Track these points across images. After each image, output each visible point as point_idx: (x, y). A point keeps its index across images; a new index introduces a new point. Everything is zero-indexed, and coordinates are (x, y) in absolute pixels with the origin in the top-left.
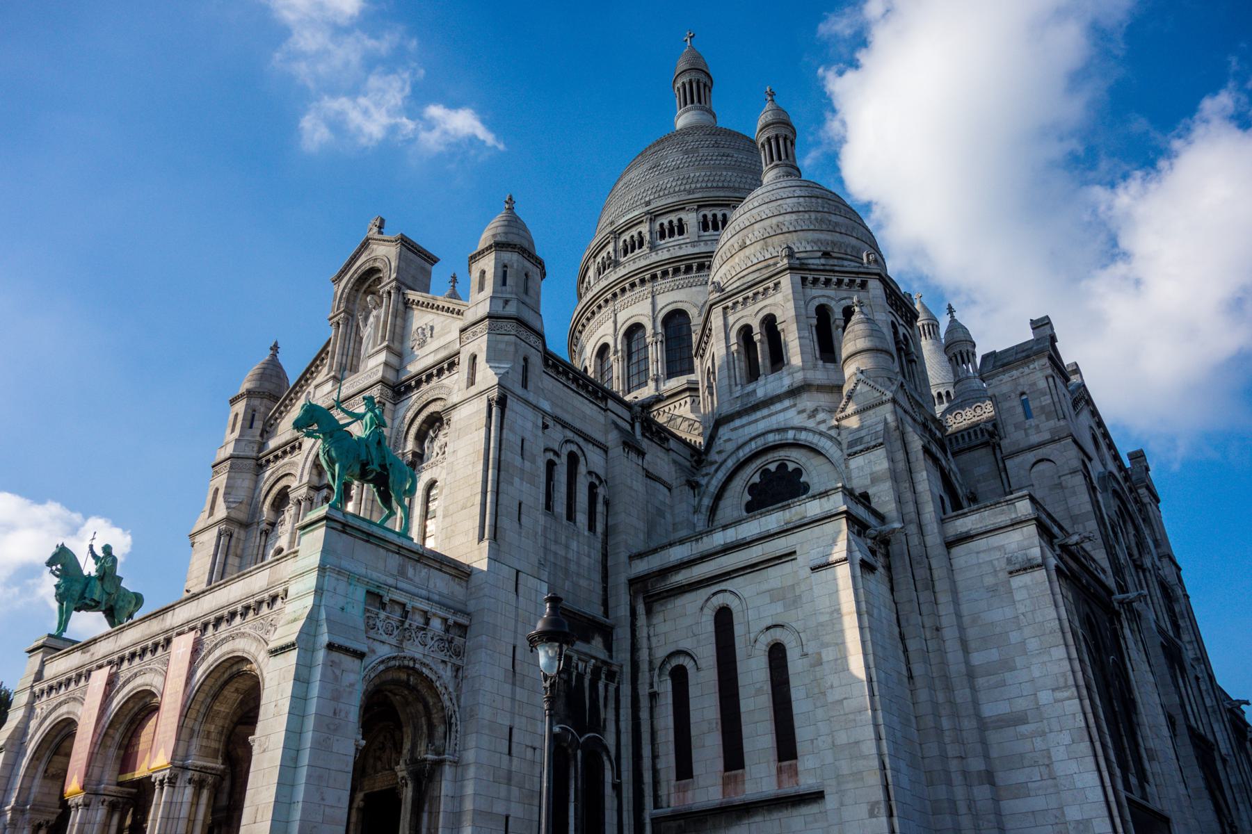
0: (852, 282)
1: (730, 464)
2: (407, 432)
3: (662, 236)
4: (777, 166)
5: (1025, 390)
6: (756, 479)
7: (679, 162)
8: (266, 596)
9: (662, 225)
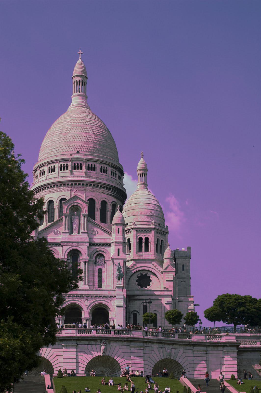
0: (164, 234)
1: (135, 271)
2: (93, 255)
3: (88, 169)
4: (143, 184)
5: (184, 264)
6: (140, 275)
7: (93, 139)
8: (110, 296)
9: (89, 165)
